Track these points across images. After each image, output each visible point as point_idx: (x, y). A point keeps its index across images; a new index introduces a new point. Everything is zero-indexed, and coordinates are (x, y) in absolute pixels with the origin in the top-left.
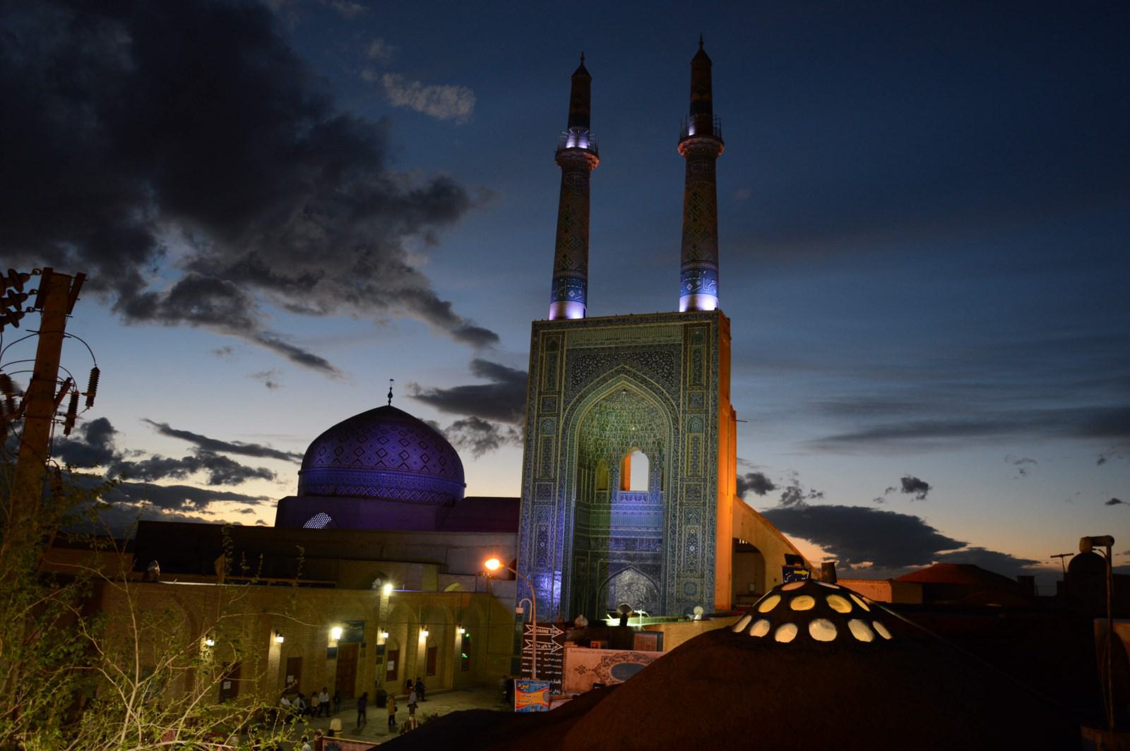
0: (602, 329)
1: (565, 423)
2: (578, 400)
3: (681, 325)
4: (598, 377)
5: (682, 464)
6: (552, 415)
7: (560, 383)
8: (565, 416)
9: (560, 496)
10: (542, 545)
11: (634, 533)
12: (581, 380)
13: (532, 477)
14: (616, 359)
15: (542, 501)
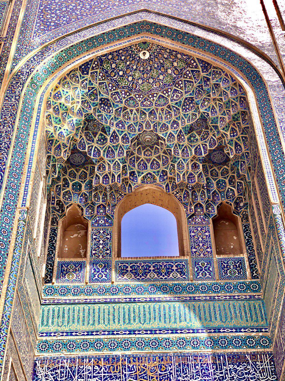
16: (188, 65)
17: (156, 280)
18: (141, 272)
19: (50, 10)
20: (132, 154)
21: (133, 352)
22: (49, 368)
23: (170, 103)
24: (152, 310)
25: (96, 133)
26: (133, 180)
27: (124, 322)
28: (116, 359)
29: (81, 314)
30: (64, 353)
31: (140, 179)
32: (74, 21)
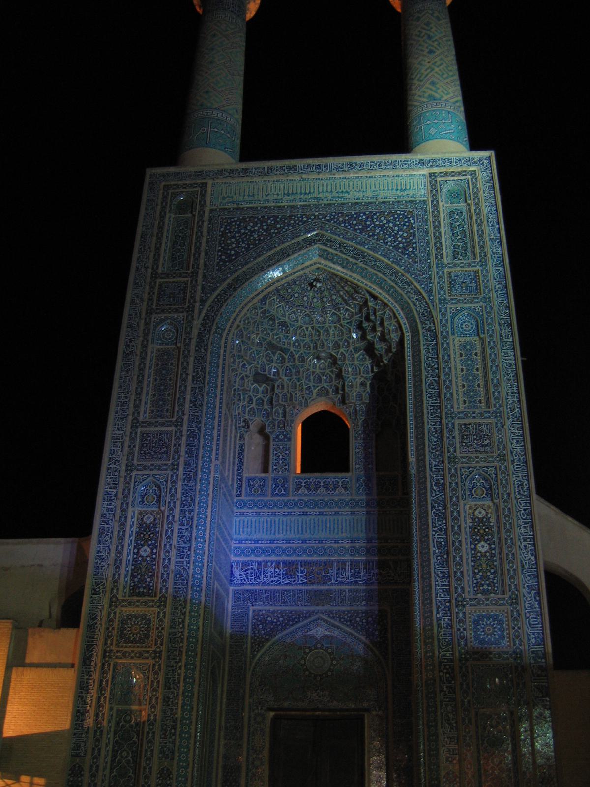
0: (278, 181)
1: (204, 325)
2: (230, 286)
3: (424, 175)
4: (271, 249)
5: (448, 387)
6: (176, 311)
7: (197, 259)
8: (204, 312)
9: (189, 453)
10: (145, 551)
11: (324, 552)
12: (237, 254)
13: (130, 418)
14: (305, 222)
15: (148, 463)
16: (356, 292)
17: (324, 495)
18: (312, 487)
19: (230, 232)
20: (308, 370)
21: (304, 558)
22: (242, 569)
23: (342, 322)
24: (320, 523)
25: (276, 353)
26: (309, 394)
27: (298, 532)
28: (291, 563)
29: (265, 525)
30: (253, 558)
31: (315, 391)
32: (252, 248)
